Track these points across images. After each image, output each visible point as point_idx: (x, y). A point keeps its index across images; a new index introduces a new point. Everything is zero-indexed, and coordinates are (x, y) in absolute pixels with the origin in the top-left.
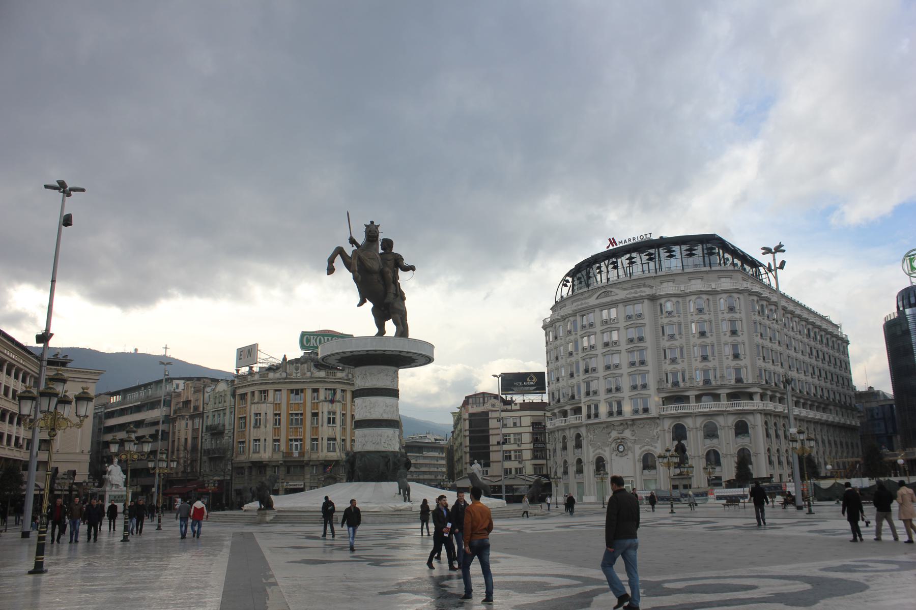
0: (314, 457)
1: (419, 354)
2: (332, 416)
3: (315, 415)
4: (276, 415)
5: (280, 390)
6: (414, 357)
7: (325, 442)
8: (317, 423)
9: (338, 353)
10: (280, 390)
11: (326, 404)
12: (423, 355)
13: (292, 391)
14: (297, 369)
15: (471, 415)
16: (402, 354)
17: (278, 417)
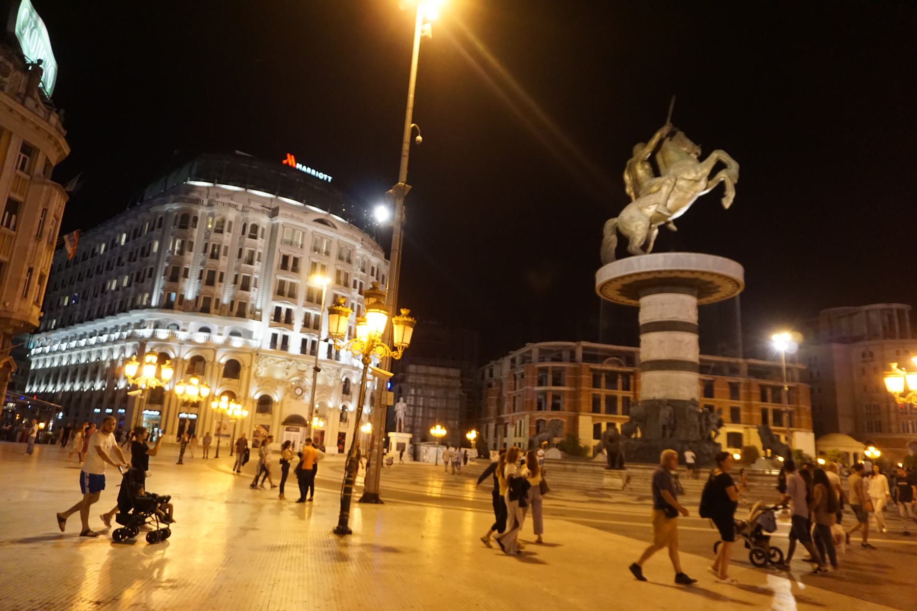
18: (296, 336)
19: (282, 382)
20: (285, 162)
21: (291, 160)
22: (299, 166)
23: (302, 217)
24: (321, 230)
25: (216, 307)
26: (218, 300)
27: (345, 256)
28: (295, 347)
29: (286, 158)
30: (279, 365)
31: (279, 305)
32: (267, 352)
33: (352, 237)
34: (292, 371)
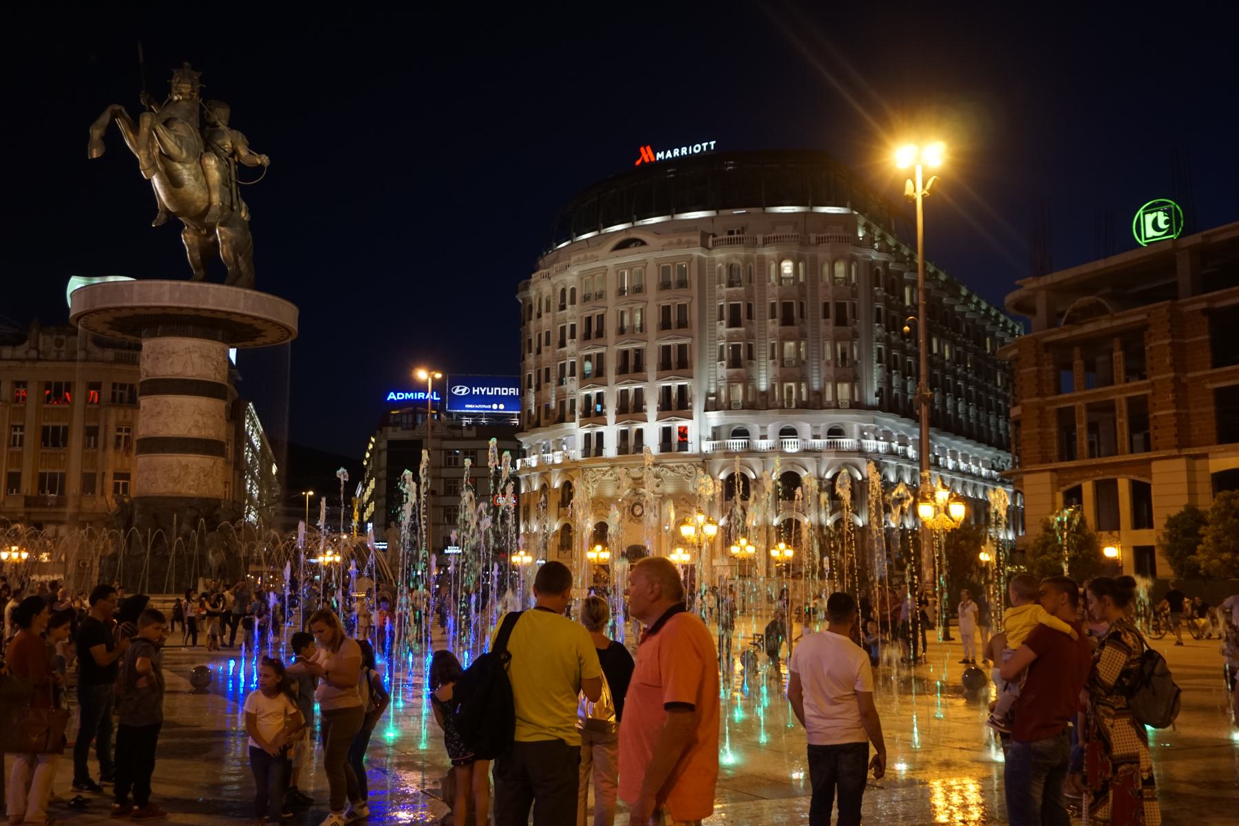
0: (87, 505)
1: (266, 321)
2: (124, 434)
3: (91, 432)
4: (15, 428)
5: (24, 384)
6: (259, 325)
7: (110, 481)
8: (96, 445)
9: (107, 310)
10: (24, 384)
11: (113, 411)
12: (274, 324)
13: (48, 385)
14: (59, 343)
15: (391, 444)
16: (234, 318)
17: (18, 433)
18: (611, 432)
19: (613, 500)
20: (638, 162)
21: (647, 155)
22: (660, 155)
23: (595, 253)
24: (631, 257)
25: (547, 417)
26: (547, 406)
27: (674, 277)
28: (610, 449)
29: (640, 155)
30: (607, 477)
31: (588, 392)
32: (584, 462)
33: (680, 244)
34: (626, 482)
